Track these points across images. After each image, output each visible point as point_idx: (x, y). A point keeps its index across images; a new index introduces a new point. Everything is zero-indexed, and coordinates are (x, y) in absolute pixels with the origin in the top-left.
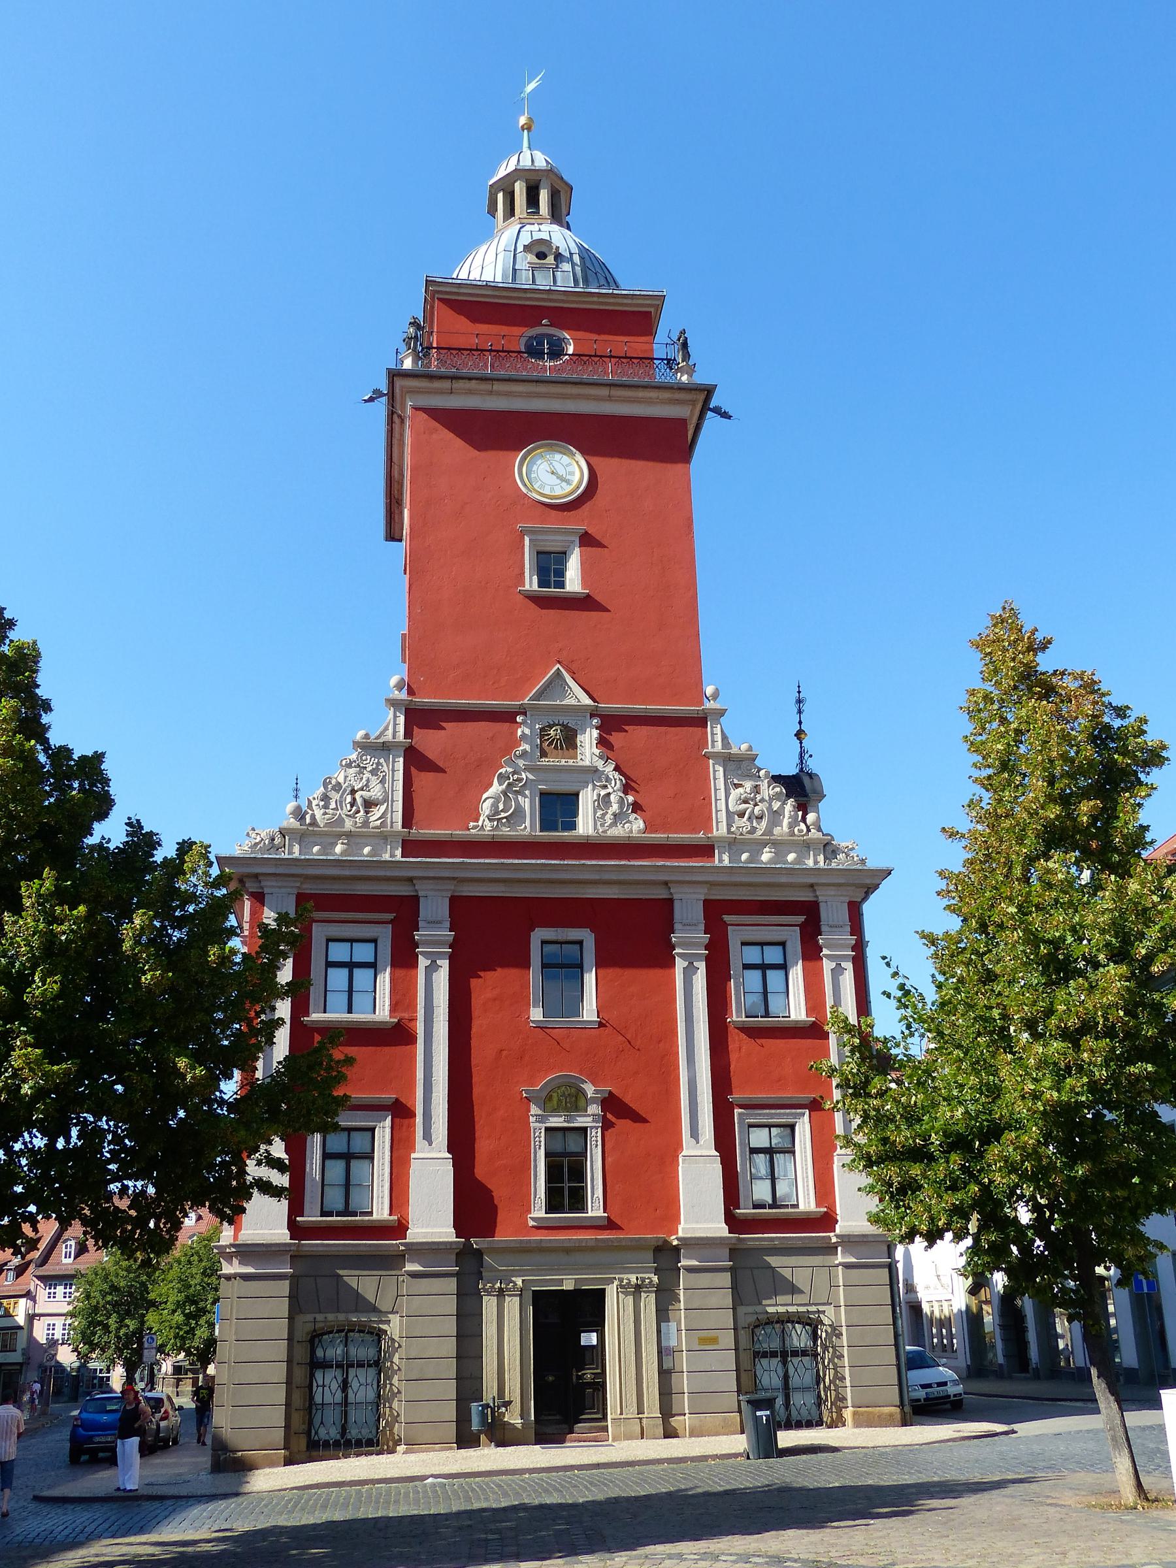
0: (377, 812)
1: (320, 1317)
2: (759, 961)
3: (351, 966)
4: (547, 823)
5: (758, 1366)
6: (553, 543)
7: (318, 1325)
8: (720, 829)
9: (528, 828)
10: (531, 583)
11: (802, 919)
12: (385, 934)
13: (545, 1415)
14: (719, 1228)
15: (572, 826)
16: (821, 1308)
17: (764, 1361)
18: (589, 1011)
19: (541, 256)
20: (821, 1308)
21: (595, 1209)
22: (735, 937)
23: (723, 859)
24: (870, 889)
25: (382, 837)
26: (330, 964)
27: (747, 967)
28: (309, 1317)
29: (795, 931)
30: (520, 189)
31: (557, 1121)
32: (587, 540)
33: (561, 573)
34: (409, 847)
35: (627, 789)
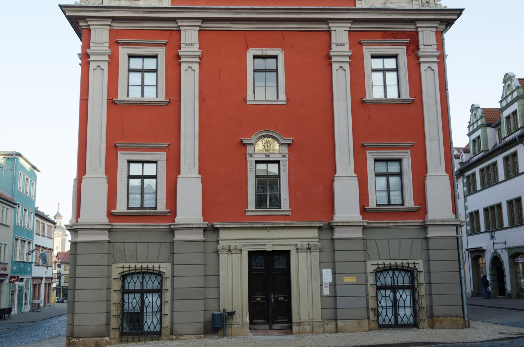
1: (126, 265)
2: (381, 67)
5: (379, 294)
7: (125, 270)
11: (407, 41)
13: (256, 319)
14: (357, 217)
16: (416, 261)
17: (383, 292)
20: (416, 261)
22: (367, 52)
24: (449, 23)
26: (130, 70)
27: (374, 70)
28: (121, 265)
29: (402, 50)
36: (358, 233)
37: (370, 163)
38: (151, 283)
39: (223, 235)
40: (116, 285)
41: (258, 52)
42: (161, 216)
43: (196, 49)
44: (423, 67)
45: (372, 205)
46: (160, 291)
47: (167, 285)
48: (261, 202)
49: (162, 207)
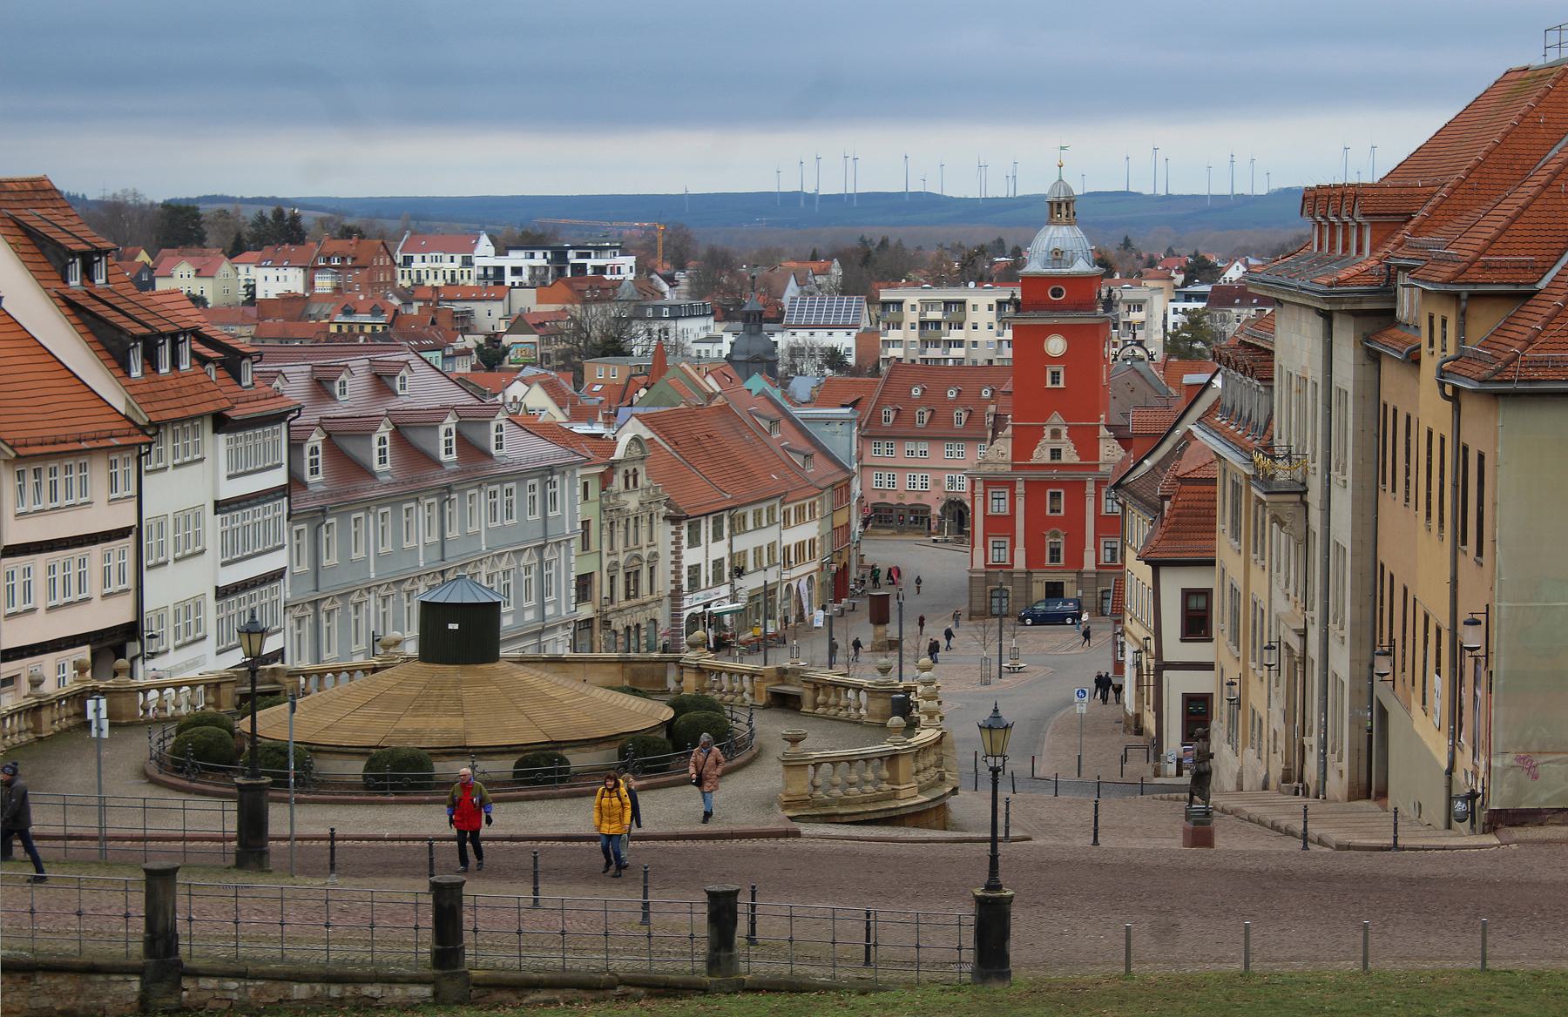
3: (999, 499)
4: (1052, 458)
6: (1056, 368)
8: (1101, 460)
9: (1047, 459)
10: (1049, 385)
12: (1007, 491)
14: (1094, 568)
15: (1060, 458)
18: (1063, 512)
21: (1062, 563)
30: (1055, 206)
31: (1052, 540)
33: (1058, 378)
34: (1014, 467)
36: (1094, 576)
37: (1102, 544)
38: (1005, 594)
39: (1034, 575)
40: (989, 595)
41: (1052, 490)
42: (1007, 566)
43: (1023, 491)
45: (1102, 563)
46: (1007, 597)
47: (1010, 595)
48: (1052, 560)
49: (1008, 563)
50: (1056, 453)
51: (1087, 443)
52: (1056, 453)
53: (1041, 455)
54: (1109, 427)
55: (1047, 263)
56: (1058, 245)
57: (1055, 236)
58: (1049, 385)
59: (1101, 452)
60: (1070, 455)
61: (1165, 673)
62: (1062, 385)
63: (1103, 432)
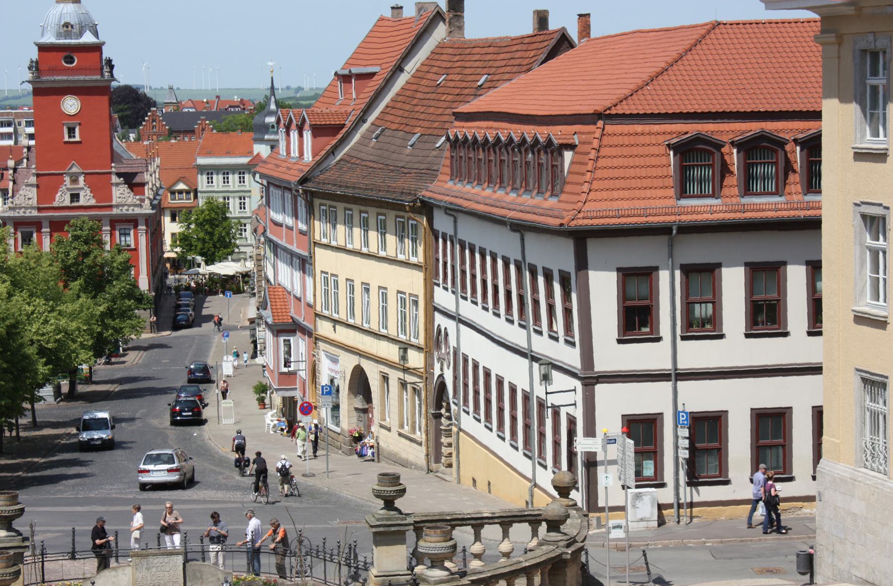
0: (31, 201)
4: (72, 201)
9: (67, 202)
19: (67, 27)
23: (115, 211)
25: (33, 208)
32: (80, 124)
33: (74, 133)
35: (91, 192)
44: (140, 234)
50: (75, 197)
51: (101, 190)
52: (75, 197)
53: (62, 198)
54: (119, 175)
55: (59, 35)
56: (68, 20)
57: (65, 11)
58: (66, 139)
59: (114, 196)
60: (86, 198)
61: (600, 389)
62: (77, 139)
63: (115, 179)
